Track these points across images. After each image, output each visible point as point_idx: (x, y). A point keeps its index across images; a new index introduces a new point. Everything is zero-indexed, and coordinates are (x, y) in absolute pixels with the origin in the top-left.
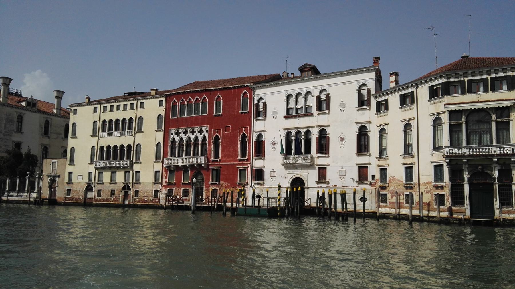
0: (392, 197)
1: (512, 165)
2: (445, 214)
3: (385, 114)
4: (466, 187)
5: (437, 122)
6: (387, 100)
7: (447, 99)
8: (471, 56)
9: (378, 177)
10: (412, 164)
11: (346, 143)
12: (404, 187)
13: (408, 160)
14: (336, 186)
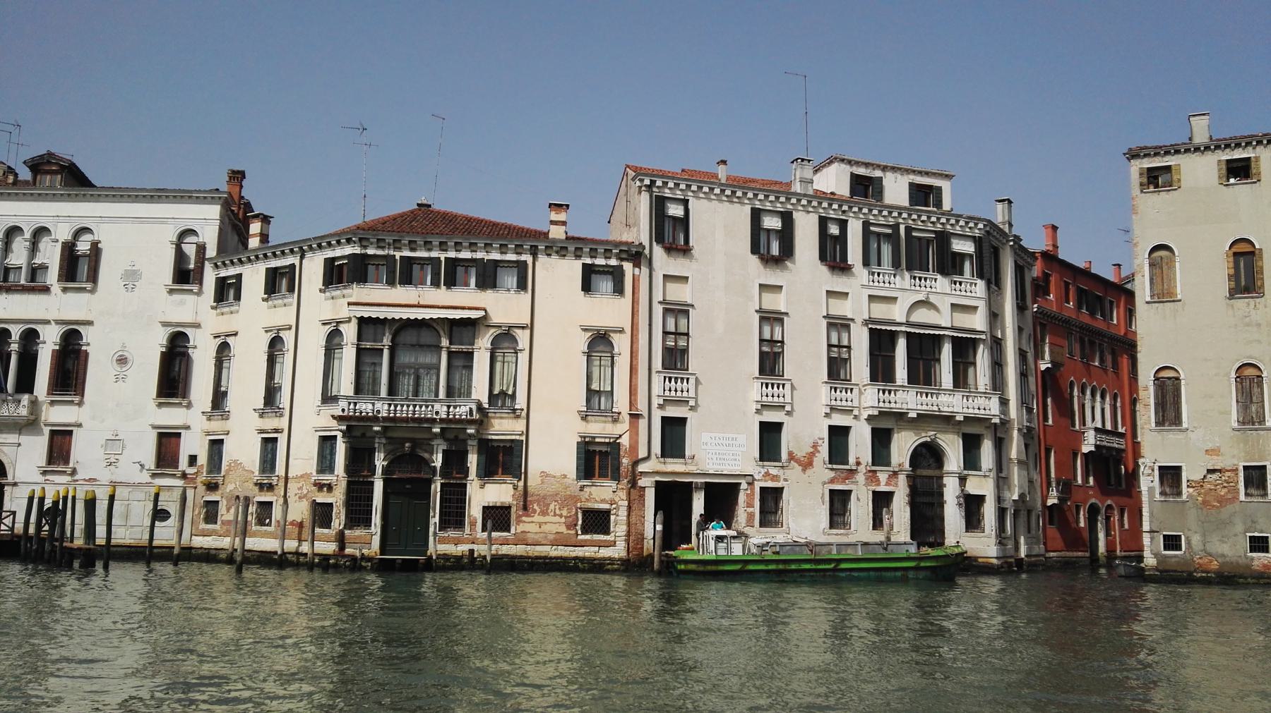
0: (228, 511)
1: (470, 442)
2: (329, 548)
3: (233, 308)
4: (378, 486)
5: (333, 341)
6: (239, 277)
7: (357, 292)
8: (437, 207)
9: (203, 460)
10: (276, 431)
11: (132, 372)
12: (256, 484)
13: (271, 423)
14: (95, 480)
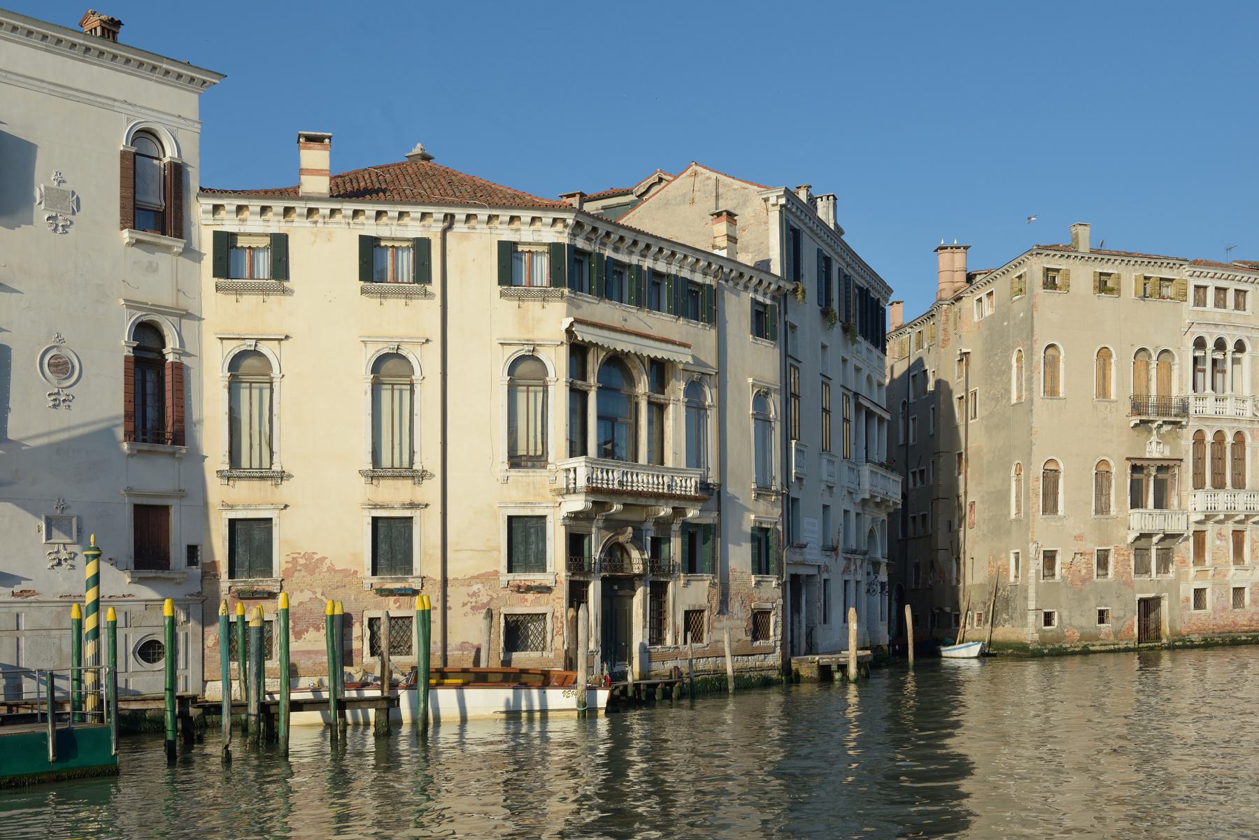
10: (412, 506)
